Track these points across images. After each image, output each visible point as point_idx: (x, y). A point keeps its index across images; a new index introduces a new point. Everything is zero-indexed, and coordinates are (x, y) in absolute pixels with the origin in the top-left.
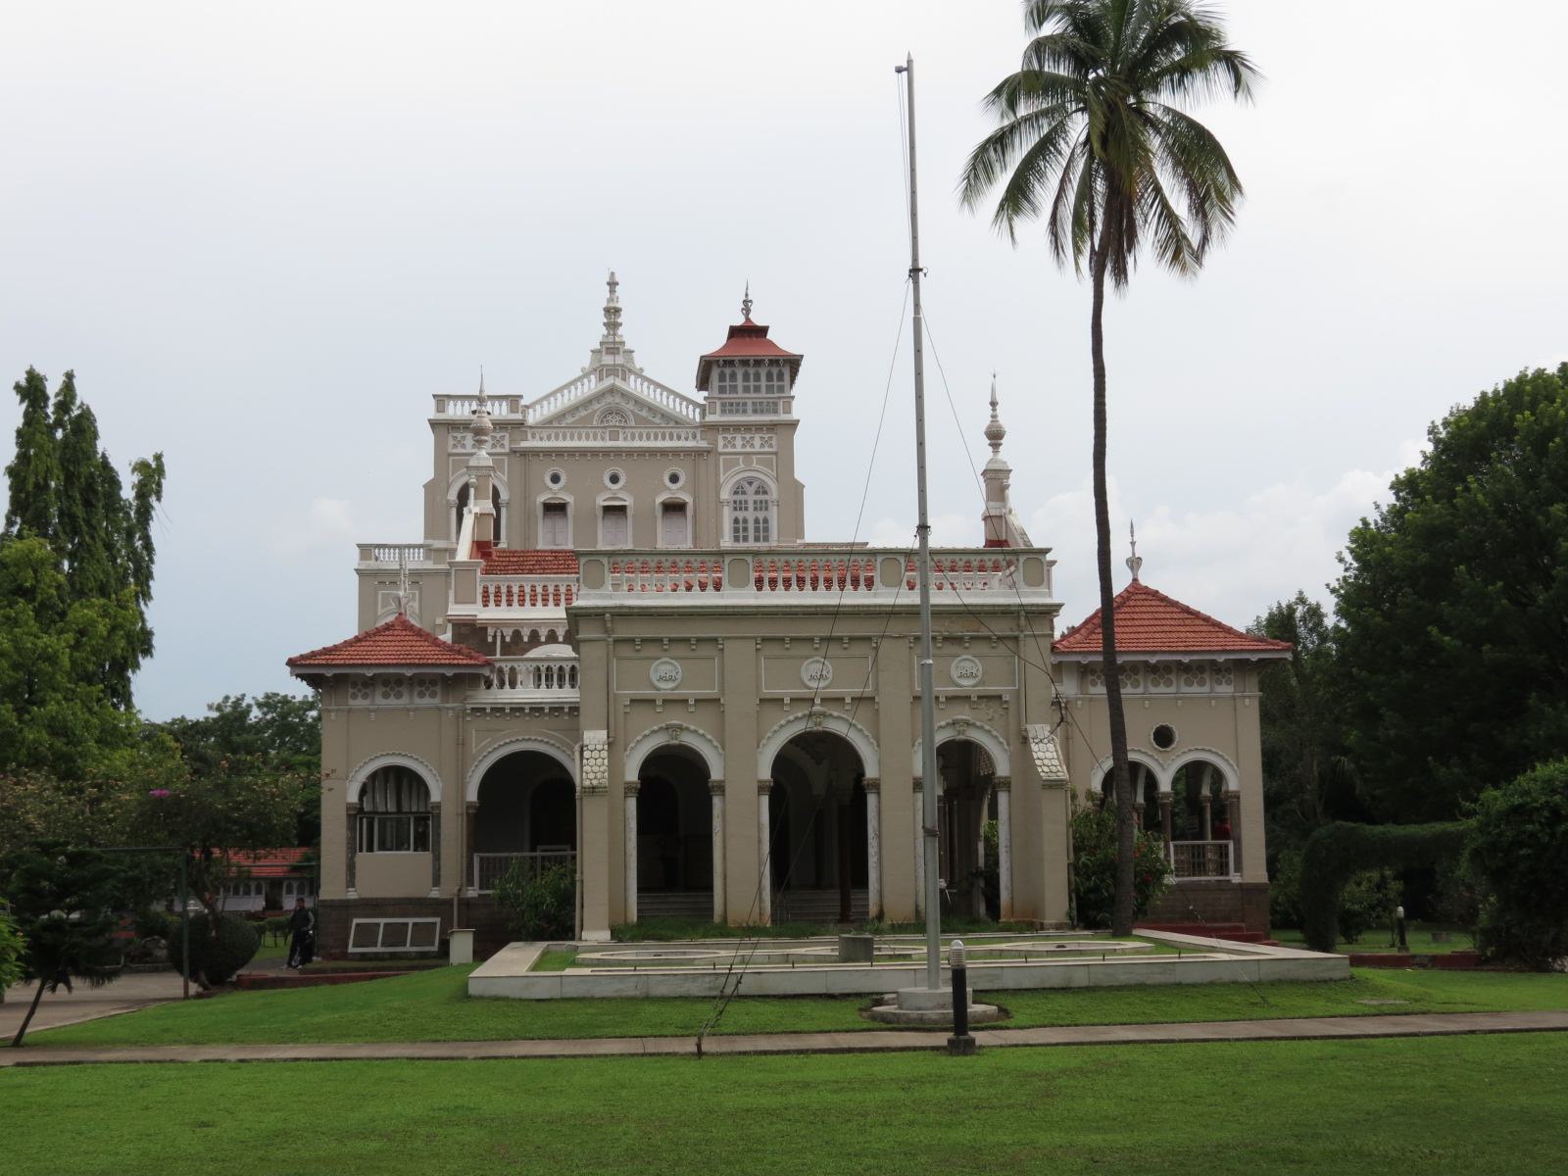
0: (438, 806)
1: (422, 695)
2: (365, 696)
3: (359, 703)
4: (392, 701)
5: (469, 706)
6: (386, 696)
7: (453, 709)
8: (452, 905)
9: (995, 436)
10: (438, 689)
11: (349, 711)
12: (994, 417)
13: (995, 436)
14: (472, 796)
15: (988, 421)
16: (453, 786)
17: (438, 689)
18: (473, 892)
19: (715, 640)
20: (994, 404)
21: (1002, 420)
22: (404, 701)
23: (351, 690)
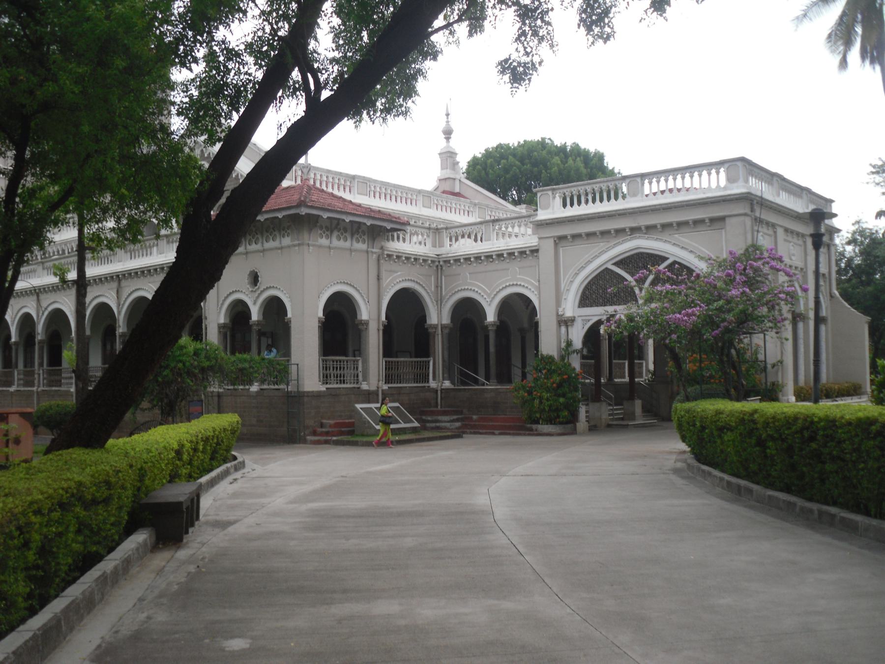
0: (367, 323)
1: (358, 242)
2: (327, 237)
3: (324, 241)
4: (341, 244)
5: (386, 252)
6: (339, 239)
7: (375, 253)
8: (378, 395)
9: (448, 133)
10: (366, 237)
11: (320, 246)
12: (448, 122)
13: (448, 133)
14: (383, 318)
15: (444, 125)
16: (371, 312)
17: (366, 237)
18: (385, 387)
19: (774, 226)
20: (448, 115)
21: (453, 125)
22: (347, 244)
23: (320, 232)
